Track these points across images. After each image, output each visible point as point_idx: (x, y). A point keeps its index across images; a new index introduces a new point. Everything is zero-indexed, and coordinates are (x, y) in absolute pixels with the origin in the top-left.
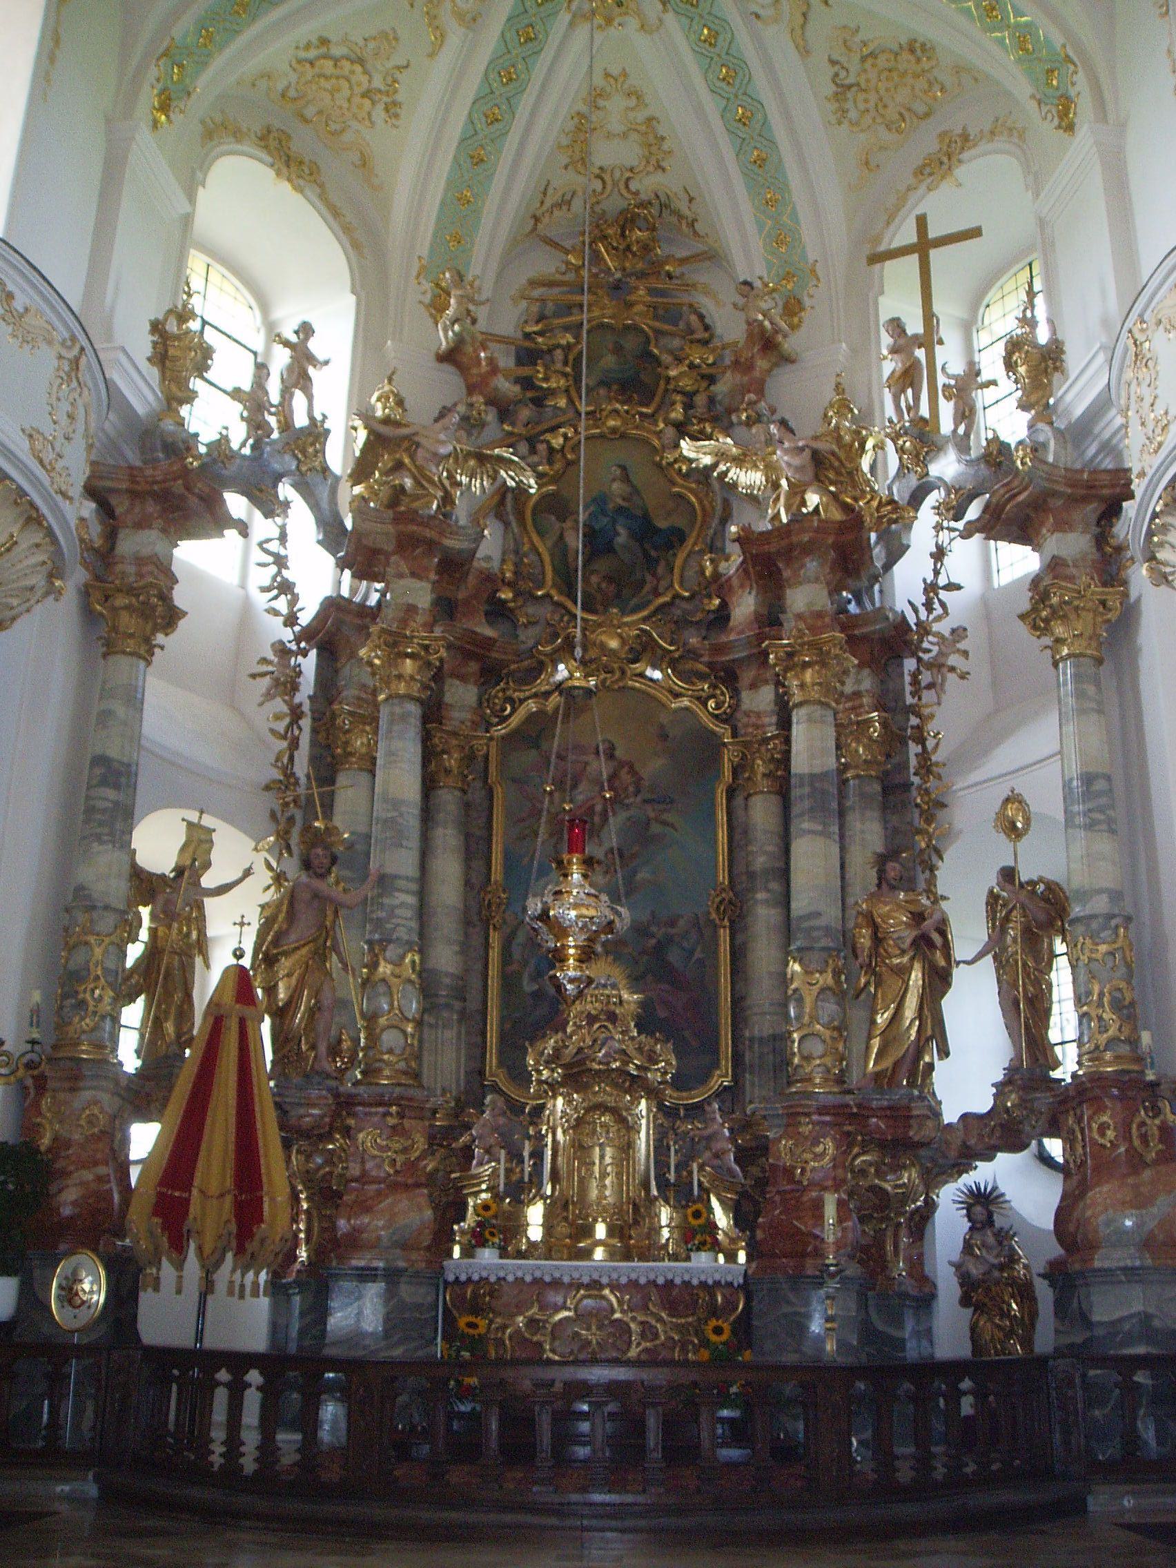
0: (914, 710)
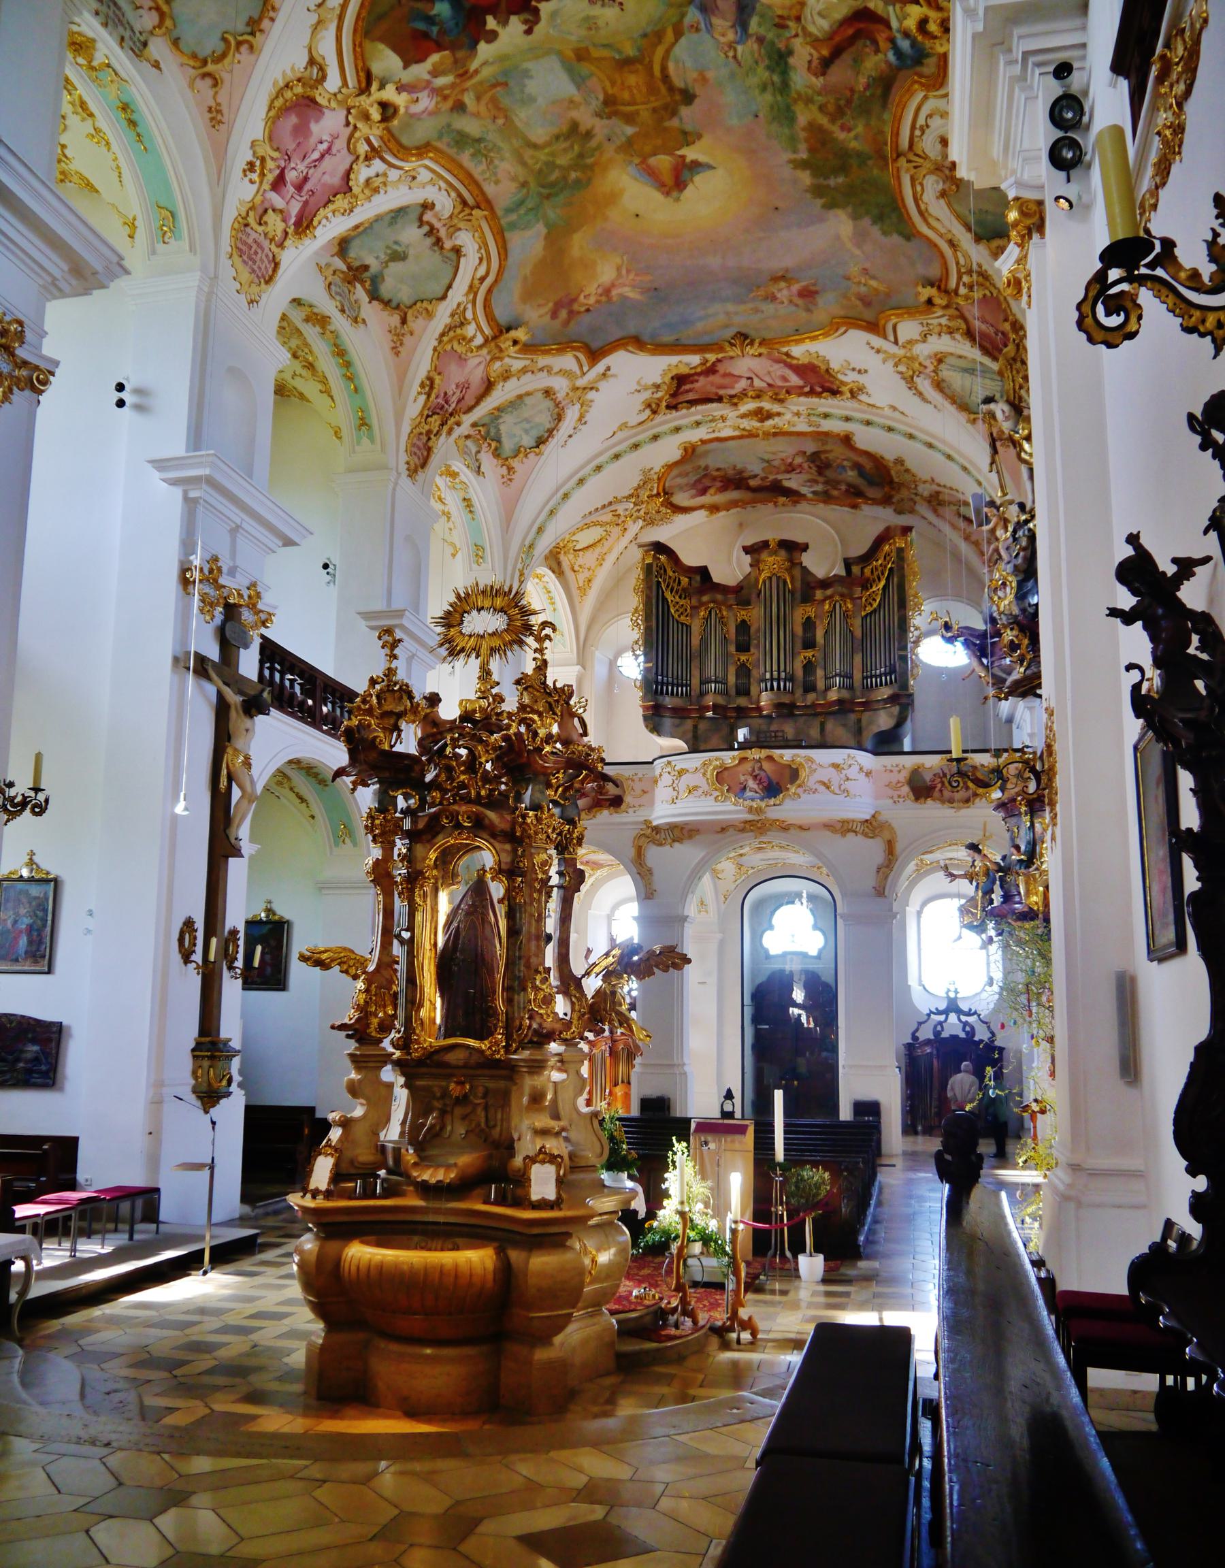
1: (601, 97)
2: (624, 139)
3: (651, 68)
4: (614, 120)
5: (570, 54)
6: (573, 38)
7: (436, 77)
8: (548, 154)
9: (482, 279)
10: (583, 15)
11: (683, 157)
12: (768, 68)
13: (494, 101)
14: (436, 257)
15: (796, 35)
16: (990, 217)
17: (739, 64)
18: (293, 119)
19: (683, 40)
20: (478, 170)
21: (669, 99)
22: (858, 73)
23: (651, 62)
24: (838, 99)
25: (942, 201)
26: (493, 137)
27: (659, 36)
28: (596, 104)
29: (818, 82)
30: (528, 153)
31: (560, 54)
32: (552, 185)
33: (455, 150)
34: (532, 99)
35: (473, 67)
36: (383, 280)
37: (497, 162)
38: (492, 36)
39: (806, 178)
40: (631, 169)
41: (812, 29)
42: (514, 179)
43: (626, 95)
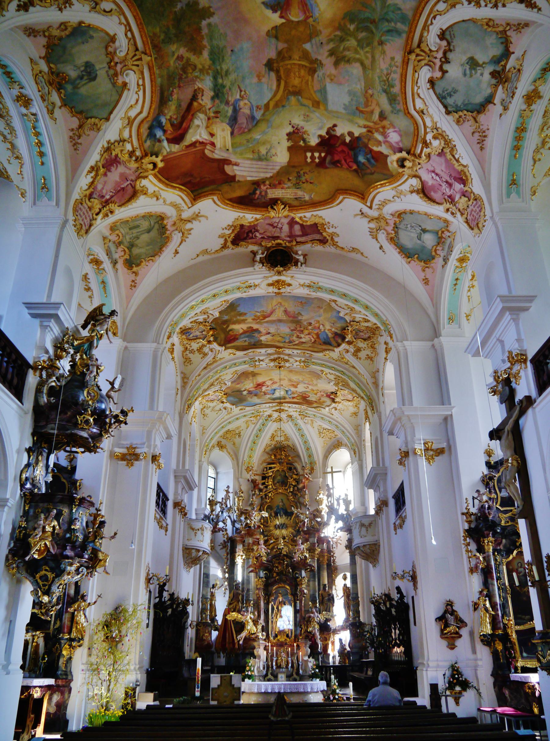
0: (332, 552)
1: (316, 76)
2: (313, 41)
3: (285, 87)
4: (314, 56)
5: (322, 107)
7: (380, 141)
10: (308, 123)
11: (281, 17)
13: (366, 106)
14: (454, 43)
15: (209, 109)
17: (239, 87)
18: (432, 193)
19: (265, 102)
20: (396, 77)
21: (281, 64)
22: (178, 99)
23: (284, 91)
24: (187, 77)
26: (378, 87)
27: (276, 105)
28: (320, 73)
29: (199, 85)
30: (367, 62)
31: (326, 109)
32: (367, 29)
33: (398, 98)
34: (350, 93)
35: (364, 130)
36: (494, 56)
37: (385, 72)
38: (350, 134)
41: (202, 116)
42: (384, 52)
43: (303, 72)
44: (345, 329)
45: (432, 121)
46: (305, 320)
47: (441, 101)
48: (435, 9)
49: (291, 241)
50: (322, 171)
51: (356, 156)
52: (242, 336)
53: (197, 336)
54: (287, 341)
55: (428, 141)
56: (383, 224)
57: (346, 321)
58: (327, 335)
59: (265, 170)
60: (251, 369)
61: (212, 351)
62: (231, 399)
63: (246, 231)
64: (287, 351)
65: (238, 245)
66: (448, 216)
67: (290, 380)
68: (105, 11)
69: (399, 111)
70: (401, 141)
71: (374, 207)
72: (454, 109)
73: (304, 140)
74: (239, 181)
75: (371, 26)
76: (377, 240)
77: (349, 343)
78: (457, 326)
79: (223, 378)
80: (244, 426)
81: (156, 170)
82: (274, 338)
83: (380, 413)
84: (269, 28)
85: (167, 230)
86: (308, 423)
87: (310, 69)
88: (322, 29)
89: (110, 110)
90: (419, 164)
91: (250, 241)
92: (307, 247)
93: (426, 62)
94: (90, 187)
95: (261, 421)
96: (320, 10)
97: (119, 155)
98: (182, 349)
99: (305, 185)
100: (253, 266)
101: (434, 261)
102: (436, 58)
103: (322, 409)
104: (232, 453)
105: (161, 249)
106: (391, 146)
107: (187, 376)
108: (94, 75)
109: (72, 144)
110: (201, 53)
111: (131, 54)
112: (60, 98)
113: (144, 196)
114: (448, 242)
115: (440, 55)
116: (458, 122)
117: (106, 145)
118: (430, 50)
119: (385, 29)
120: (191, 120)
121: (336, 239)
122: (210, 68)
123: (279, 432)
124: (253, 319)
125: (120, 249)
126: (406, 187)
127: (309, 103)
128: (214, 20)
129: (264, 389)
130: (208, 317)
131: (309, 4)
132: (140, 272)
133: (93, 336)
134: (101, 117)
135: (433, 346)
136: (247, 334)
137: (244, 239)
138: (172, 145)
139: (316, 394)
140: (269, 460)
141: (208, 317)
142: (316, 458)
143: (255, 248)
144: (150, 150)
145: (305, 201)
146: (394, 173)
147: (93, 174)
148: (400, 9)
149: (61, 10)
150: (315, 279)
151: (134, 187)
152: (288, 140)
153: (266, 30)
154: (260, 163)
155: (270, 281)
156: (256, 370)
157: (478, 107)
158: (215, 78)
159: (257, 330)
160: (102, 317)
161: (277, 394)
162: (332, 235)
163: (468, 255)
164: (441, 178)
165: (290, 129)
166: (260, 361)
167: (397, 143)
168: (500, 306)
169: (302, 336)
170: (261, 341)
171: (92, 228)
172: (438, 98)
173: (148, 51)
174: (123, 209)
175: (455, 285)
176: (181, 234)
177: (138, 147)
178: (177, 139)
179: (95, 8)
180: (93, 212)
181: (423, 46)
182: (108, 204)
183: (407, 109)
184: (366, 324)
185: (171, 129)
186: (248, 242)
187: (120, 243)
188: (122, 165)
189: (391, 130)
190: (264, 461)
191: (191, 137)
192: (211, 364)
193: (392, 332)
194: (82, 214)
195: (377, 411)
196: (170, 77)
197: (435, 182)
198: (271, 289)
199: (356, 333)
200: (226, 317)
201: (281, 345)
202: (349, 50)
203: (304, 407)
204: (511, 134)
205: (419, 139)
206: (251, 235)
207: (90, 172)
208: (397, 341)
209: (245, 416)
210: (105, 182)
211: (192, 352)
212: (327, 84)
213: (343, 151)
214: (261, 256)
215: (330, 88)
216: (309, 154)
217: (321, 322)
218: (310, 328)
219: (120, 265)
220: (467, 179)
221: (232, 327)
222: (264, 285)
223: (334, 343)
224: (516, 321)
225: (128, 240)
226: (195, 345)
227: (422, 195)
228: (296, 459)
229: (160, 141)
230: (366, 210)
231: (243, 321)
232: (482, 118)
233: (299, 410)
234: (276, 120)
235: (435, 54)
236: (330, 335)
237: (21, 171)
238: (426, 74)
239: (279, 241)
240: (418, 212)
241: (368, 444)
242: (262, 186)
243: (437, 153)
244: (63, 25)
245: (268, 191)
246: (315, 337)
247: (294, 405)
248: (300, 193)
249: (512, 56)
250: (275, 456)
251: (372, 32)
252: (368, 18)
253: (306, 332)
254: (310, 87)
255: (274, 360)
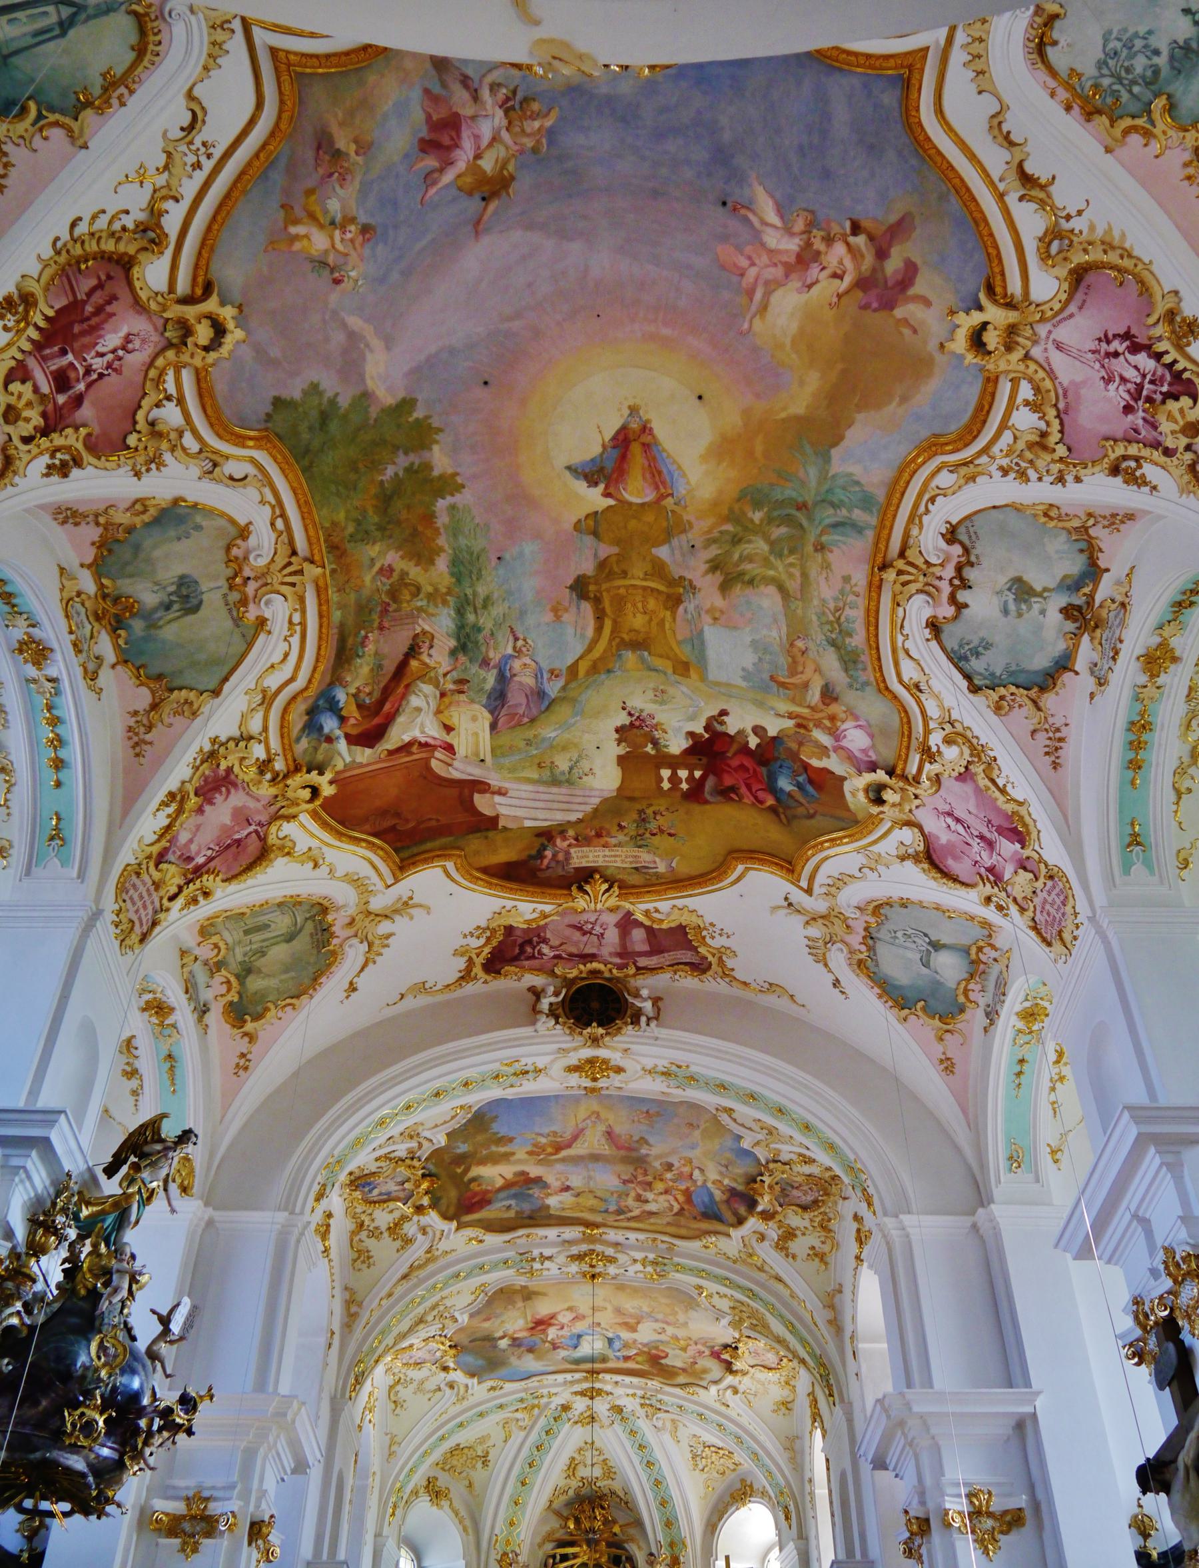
1: (681, 609)
3: (612, 632)
4: (676, 572)
5: (692, 673)
6: (685, 689)
8: (772, 567)
9: (954, 468)
11: (607, 495)
12: (479, 630)
13: (793, 671)
15: (445, 675)
16: (172, 533)
18: (950, 862)
19: (570, 662)
20: (855, 615)
21: (604, 586)
22: (376, 653)
23: (611, 641)
25: (242, 522)
26: (818, 636)
27: (594, 669)
28: (689, 605)
29: (424, 625)
30: (793, 585)
31: (703, 678)
32: (788, 520)
33: (863, 658)
35: (790, 723)
36: (1065, 577)
37: (832, 605)
38: (758, 730)
39: (440, 460)
40: (681, 490)
41: (427, 689)
42: (827, 566)
43: (652, 604)
44: (755, 1181)
45: (941, 706)
46: (657, 1157)
47: (956, 666)
48: (933, 484)
49: (625, 966)
50: (696, 808)
51: (772, 778)
52: (502, 1195)
53: (389, 1194)
54: (612, 1208)
55: (934, 749)
56: (839, 928)
57: (758, 1160)
58: (711, 1195)
59: (565, 806)
60: (522, 1281)
61: (425, 1233)
62: (469, 1359)
63: (520, 941)
64: (612, 1235)
65: (498, 972)
66: (990, 914)
67: (618, 1311)
68: (231, 478)
69: (867, 684)
70: (873, 746)
71: (817, 889)
72: (988, 682)
73: (655, 743)
74: (505, 829)
75: (798, 514)
76: (826, 965)
77: (767, 1216)
78: (1032, 1176)
79: (448, 1303)
80: (497, 1435)
81: (318, 803)
82: (580, 1200)
83: (850, 1404)
84: (582, 514)
85: (332, 935)
86: (664, 1428)
87: (669, 596)
88: (693, 520)
89: (224, 674)
90: (916, 797)
91: (526, 963)
92: (662, 980)
93: (919, 586)
94: (162, 836)
95: (542, 1421)
96: (688, 483)
97: (236, 769)
98: (350, 1225)
99: (656, 840)
100: (533, 1023)
101: (963, 1017)
102: (940, 578)
103: (701, 1391)
104: (463, 1513)
105: (315, 979)
106: (850, 757)
107: (358, 1298)
108: (194, 601)
109: (131, 743)
110: (432, 562)
111: (281, 561)
112: (117, 646)
113: (286, 859)
114: (995, 970)
115: (949, 572)
116: (998, 709)
117: (207, 747)
118: (927, 562)
119: (828, 521)
120: (404, 696)
121: (730, 963)
122: (449, 593)
123: (588, 1454)
124: (530, 1153)
125: (218, 978)
126: (889, 846)
127: (667, 666)
128: (463, 499)
129: (552, 1333)
130: (420, 1145)
131: (665, 471)
132: (261, 1034)
133: (132, 1195)
134: (201, 688)
135: (974, 1226)
136: (513, 1191)
137: (514, 960)
138: (358, 749)
139: (684, 1349)
140: (560, 1534)
141: (420, 1145)
142: (685, 1532)
143: (538, 980)
144: (307, 758)
145: (657, 875)
146: (860, 816)
147: (171, 810)
148: (857, 483)
149: (137, 474)
150: (680, 1056)
151: (263, 839)
152: (619, 742)
153: (574, 520)
154: (555, 790)
155: (573, 1059)
156: (533, 1284)
157: (1039, 680)
158: (460, 612)
159: (538, 1181)
160: (158, 1147)
161: (585, 1349)
162: (721, 953)
163: (1045, 1004)
164: (967, 828)
165: (623, 719)
166: (544, 1258)
167: (864, 751)
168: (1133, 1132)
169: (650, 1196)
170: (548, 1207)
171: (158, 929)
172: (950, 659)
173: (317, 558)
174: (233, 887)
175: (1019, 1074)
176: (365, 946)
177: (280, 751)
178: (369, 738)
179: (211, 472)
180: (162, 892)
181: (911, 554)
182: (201, 876)
183: (884, 681)
184: (807, 1169)
185: (357, 715)
186: (522, 967)
187: (219, 965)
188: (241, 792)
189: (849, 724)
190: (548, 1538)
191: (399, 734)
192: (420, 1267)
193: (871, 1190)
194: (136, 896)
195: (842, 1400)
196: (363, 609)
197: (953, 837)
198: (575, 1080)
199: (783, 1190)
200: (463, 1148)
201: (598, 1219)
202: (751, 561)
203: (654, 1384)
204: (1120, 737)
205: (914, 744)
206: (529, 950)
207: (164, 804)
208: (885, 1214)
209: (501, 1406)
210: (198, 827)
211: (375, 1233)
212: (706, 628)
213: (742, 767)
214: (553, 999)
215: (712, 635)
216: (666, 773)
217: (696, 1163)
218: (669, 1176)
219: (215, 1018)
220: (1029, 833)
221: (475, 1171)
222: (557, 1069)
223: (728, 1215)
224: (1175, 1168)
225: (239, 958)
226: (383, 1217)
227: (926, 866)
228: (632, 1531)
229: (329, 740)
230: (798, 896)
231: (506, 1157)
232: (1049, 700)
233: (640, 1393)
234: (592, 698)
235: (937, 571)
236: (718, 1195)
237: (6, 800)
238: (919, 608)
239: (595, 965)
240: (921, 905)
241: (821, 1492)
242: (558, 841)
243: (955, 774)
244: (140, 505)
245: (572, 850)
246: (681, 1198)
247: (628, 1379)
248: (645, 857)
249: (1106, 575)
250: (577, 1521)
251: (801, 526)
252: (791, 499)
253: (660, 1186)
254: (668, 632)
255: (579, 1257)
